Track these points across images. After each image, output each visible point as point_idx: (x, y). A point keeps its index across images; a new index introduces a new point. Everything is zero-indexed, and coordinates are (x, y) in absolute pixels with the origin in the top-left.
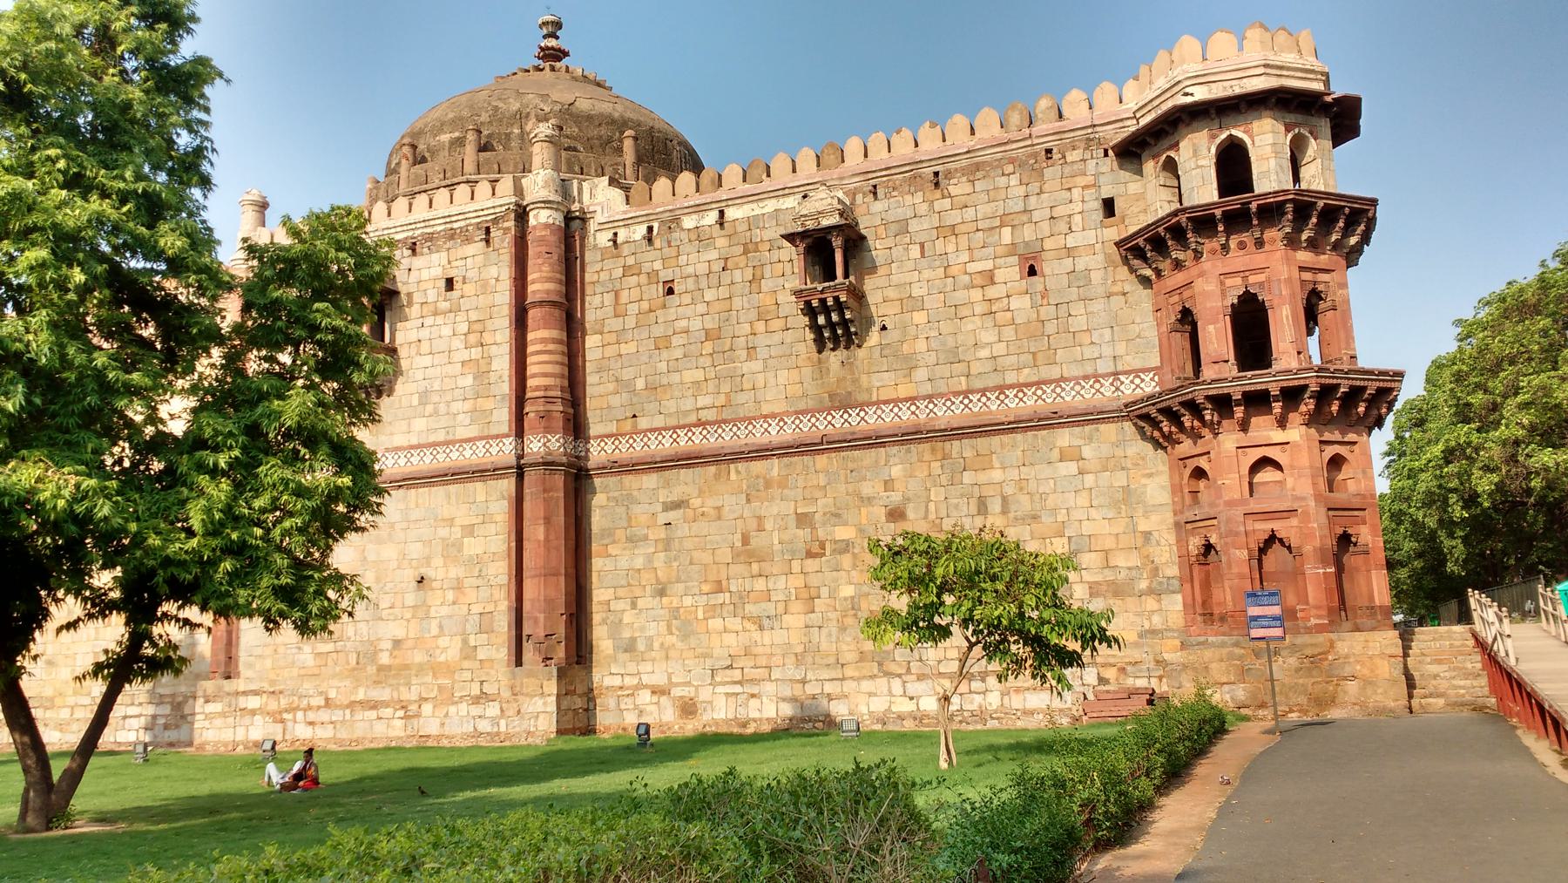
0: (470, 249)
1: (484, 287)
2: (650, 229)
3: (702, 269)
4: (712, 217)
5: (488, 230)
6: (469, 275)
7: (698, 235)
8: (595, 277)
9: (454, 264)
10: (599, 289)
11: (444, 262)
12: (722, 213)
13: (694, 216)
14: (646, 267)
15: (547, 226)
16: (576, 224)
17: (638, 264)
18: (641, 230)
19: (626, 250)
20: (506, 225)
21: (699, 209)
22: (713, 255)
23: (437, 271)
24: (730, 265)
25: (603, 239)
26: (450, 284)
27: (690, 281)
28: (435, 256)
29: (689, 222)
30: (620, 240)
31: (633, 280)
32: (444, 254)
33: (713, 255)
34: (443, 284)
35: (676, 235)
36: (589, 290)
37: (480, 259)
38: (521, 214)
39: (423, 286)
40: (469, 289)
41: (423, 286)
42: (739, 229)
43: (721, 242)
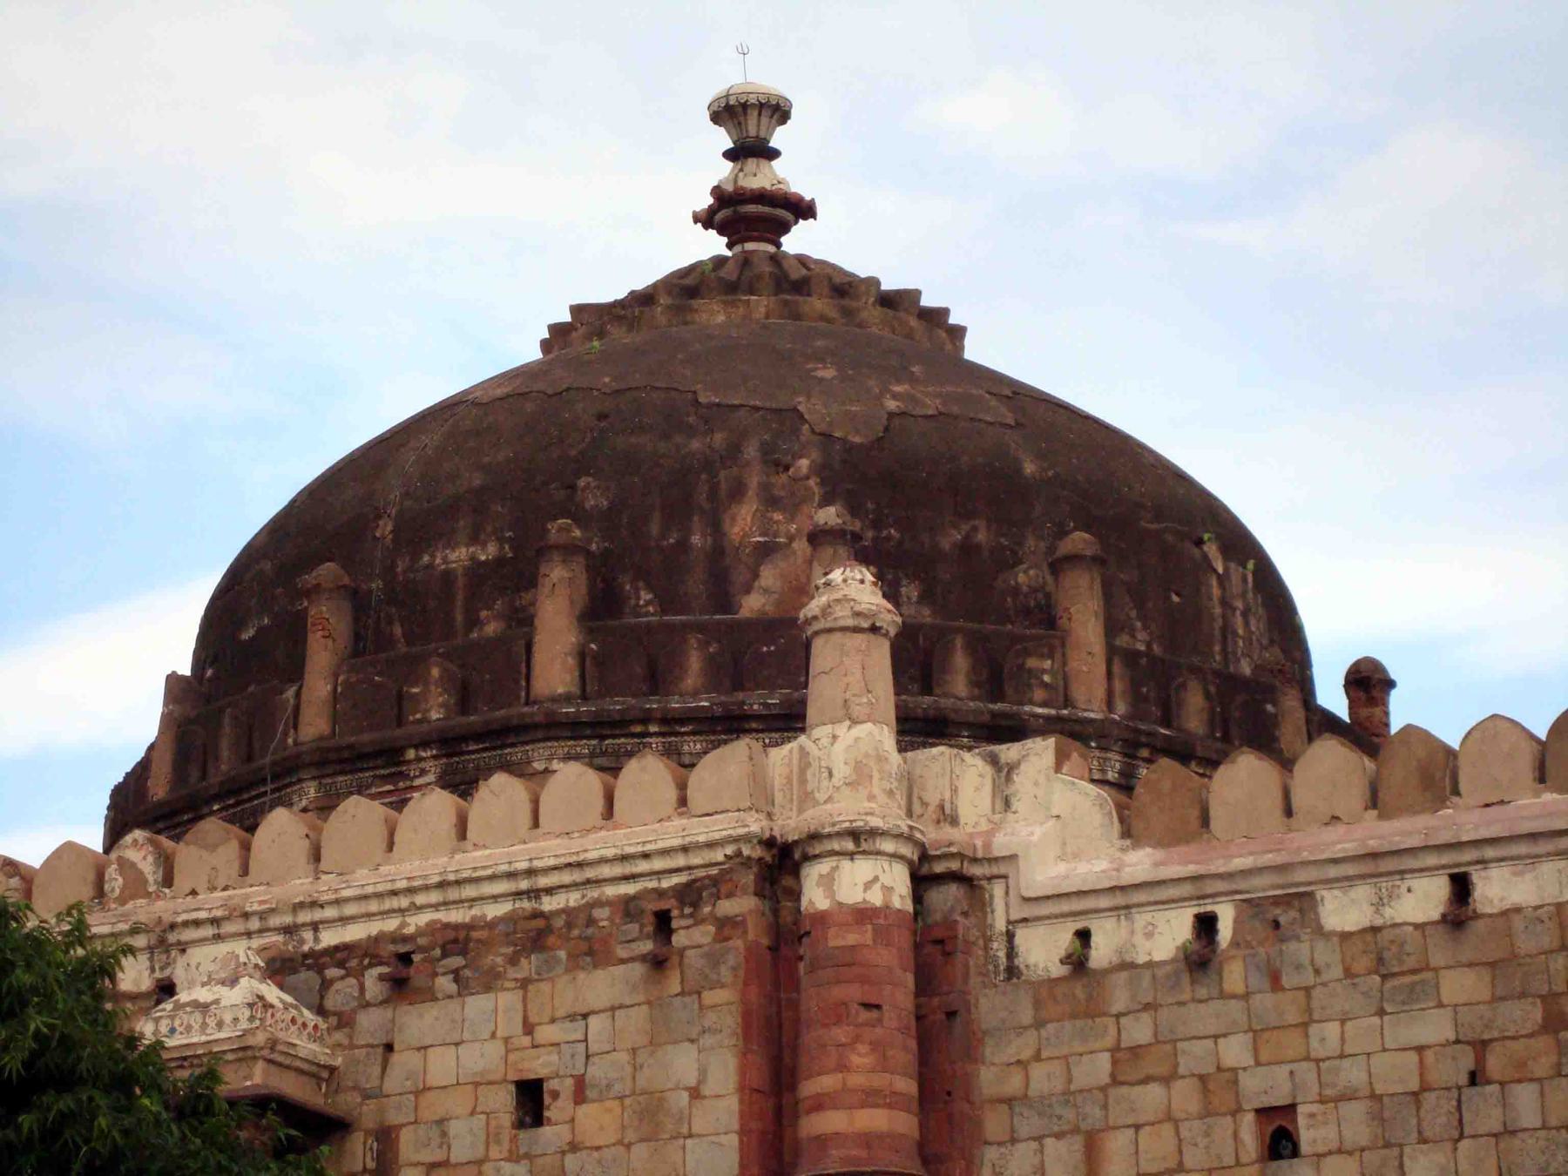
0: (600, 986)
1: (651, 1118)
2: (1206, 925)
3: (1396, 1073)
4: (1423, 899)
5: (663, 923)
6: (596, 1072)
7: (1381, 958)
8: (1014, 1084)
9: (546, 1033)
10: (1028, 1124)
11: (511, 1025)
12: (1461, 886)
13: (1363, 892)
14: (1195, 1056)
15: (863, 914)
16: (945, 898)
17: (1166, 1042)
18: (1170, 933)
19: (1120, 1000)
20: (727, 907)
21: (1379, 866)
22: (1433, 1028)
23: (483, 1057)
24: (1495, 1064)
25: (1042, 951)
26: (531, 1099)
27: (1355, 1112)
28: (478, 1004)
29: (1344, 911)
30: (1101, 952)
31: (1155, 1091)
32: (508, 1000)
33: (1433, 1028)
34: (503, 1101)
35: (1299, 949)
36: (994, 1123)
37: (635, 1021)
38: (781, 863)
39: (434, 1106)
40: (597, 1121)
41: (434, 1106)
42: (1525, 944)
43: (1461, 985)
